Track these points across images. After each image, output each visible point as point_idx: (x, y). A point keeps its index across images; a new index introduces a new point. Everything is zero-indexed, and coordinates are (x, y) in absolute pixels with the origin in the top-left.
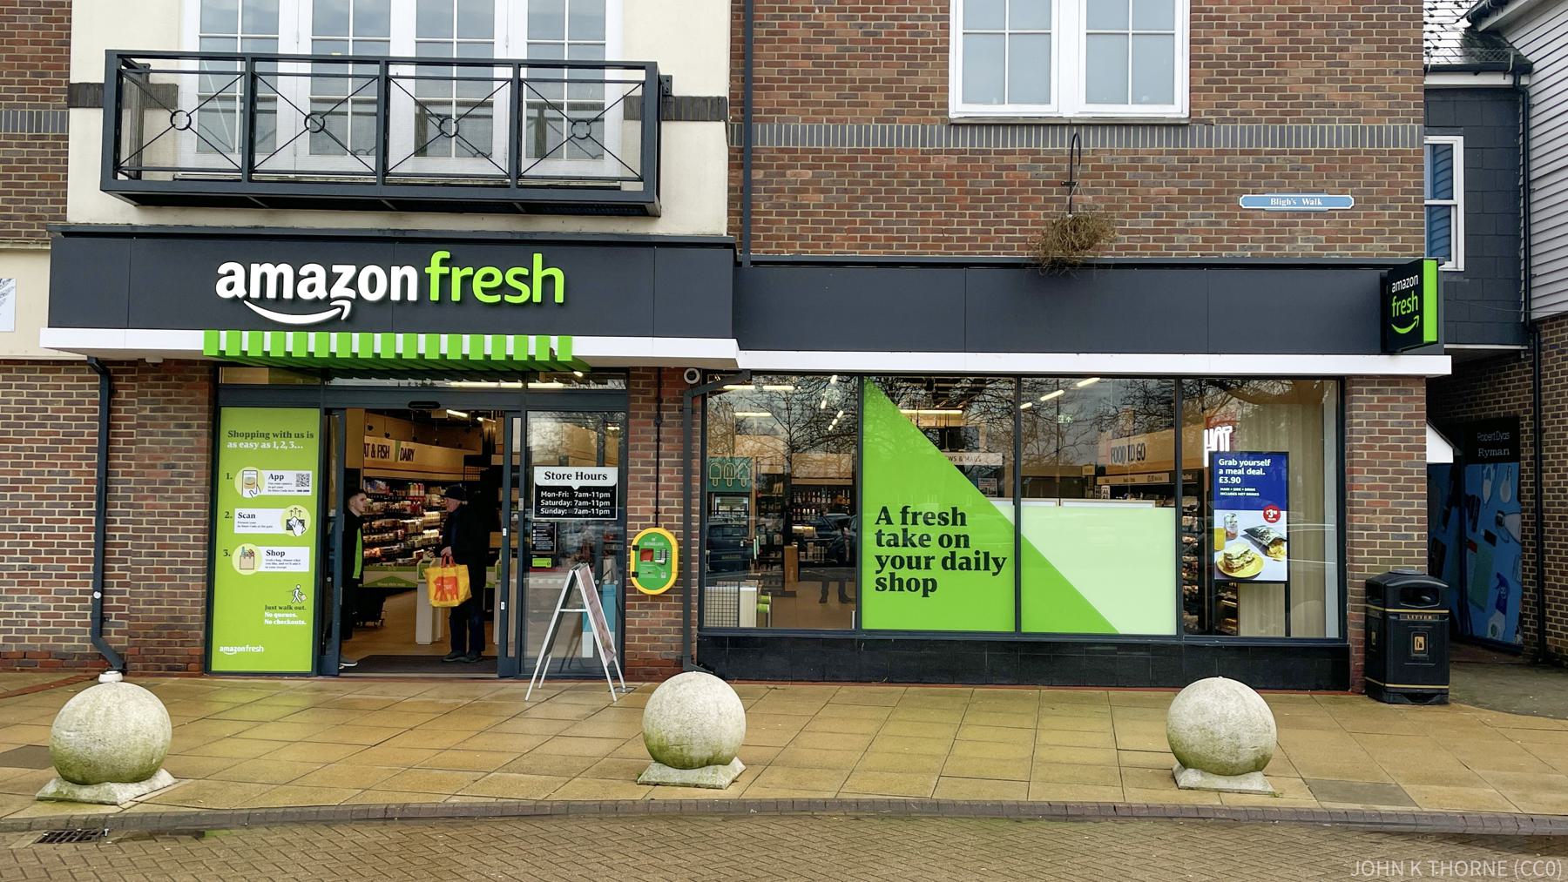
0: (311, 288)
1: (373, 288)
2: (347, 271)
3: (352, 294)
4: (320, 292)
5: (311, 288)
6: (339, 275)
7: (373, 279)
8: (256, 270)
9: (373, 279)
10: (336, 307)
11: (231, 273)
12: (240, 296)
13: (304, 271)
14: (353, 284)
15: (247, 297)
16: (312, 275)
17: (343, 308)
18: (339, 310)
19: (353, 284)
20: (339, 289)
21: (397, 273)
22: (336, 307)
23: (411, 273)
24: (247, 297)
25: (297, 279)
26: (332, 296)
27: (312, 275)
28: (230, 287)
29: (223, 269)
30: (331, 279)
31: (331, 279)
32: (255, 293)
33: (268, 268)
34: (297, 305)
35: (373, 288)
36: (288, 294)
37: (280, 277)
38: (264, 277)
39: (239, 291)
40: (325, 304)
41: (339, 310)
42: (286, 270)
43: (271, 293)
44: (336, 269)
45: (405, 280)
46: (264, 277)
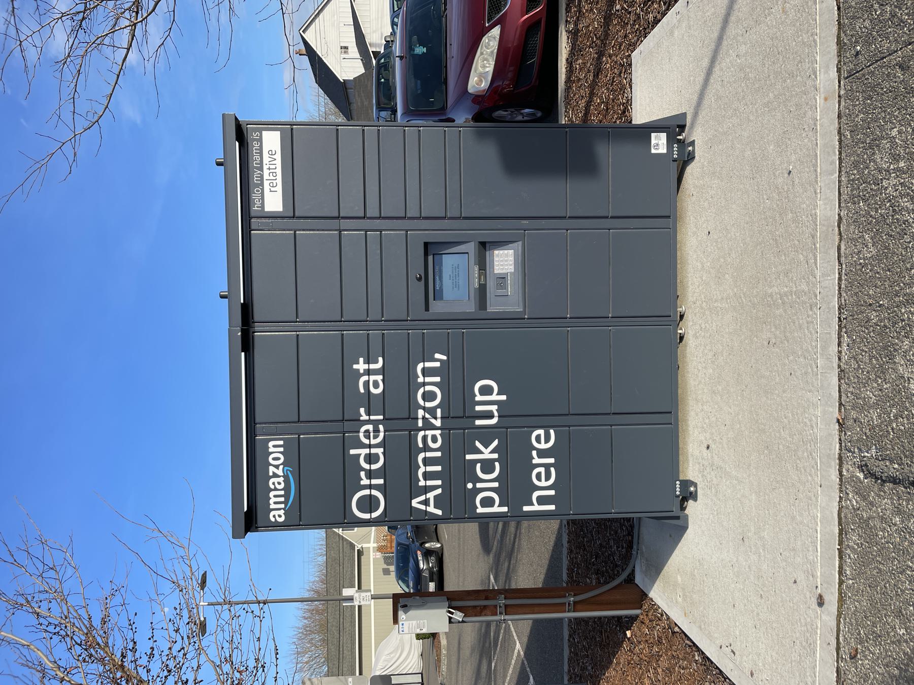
0: (279, 483)
1: (278, 459)
3: (281, 467)
4: (281, 480)
5: (279, 483)
6: (273, 472)
7: (274, 459)
9: (274, 459)
10: (287, 473)
11: (274, 516)
12: (284, 512)
13: (272, 487)
15: (284, 509)
16: (274, 484)
17: (287, 470)
18: (288, 471)
20: (280, 472)
22: (287, 471)
23: (271, 444)
24: (284, 509)
26: (282, 474)
27: (274, 484)
28: (280, 516)
29: (273, 520)
30: (275, 475)
32: (283, 506)
33: (271, 502)
34: (287, 489)
35: (278, 459)
36: (282, 493)
38: (275, 503)
40: (286, 478)
41: (288, 471)
43: (282, 499)
44: (271, 474)
45: (274, 446)
46: (275, 503)
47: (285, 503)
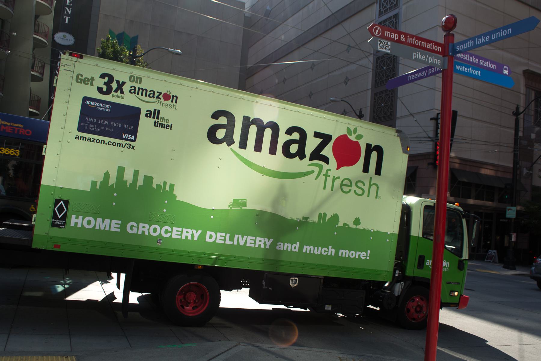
2: (96, 103)
4: (94, 104)
8: (89, 102)
14: (97, 104)
19: (97, 104)
20: (95, 104)
21: (100, 104)
25: (92, 103)
30: (95, 104)
31: (95, 104)
33: (90, 102)
37: (91, 103)
38: (89, 103)
39: (87, 103)
40: (94, 105)
42: (91, 102)
47: (89, 104)
